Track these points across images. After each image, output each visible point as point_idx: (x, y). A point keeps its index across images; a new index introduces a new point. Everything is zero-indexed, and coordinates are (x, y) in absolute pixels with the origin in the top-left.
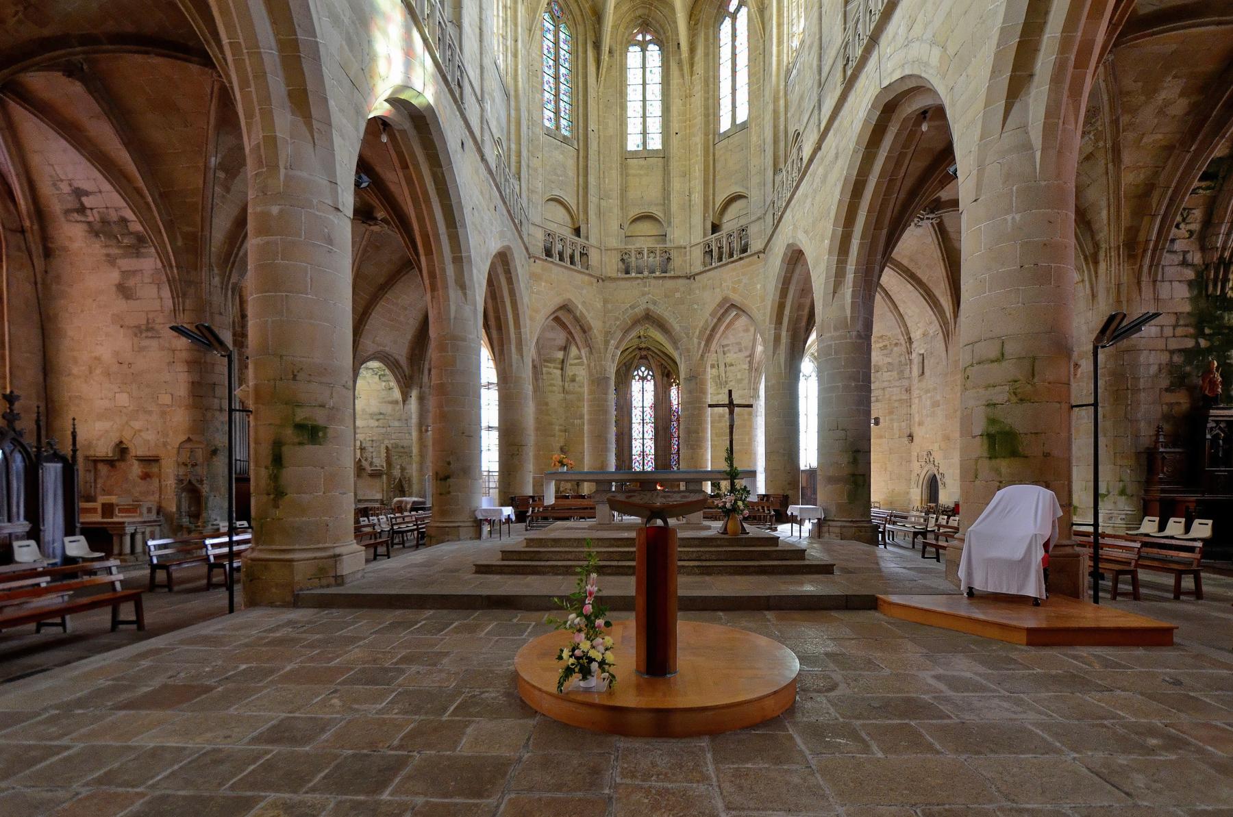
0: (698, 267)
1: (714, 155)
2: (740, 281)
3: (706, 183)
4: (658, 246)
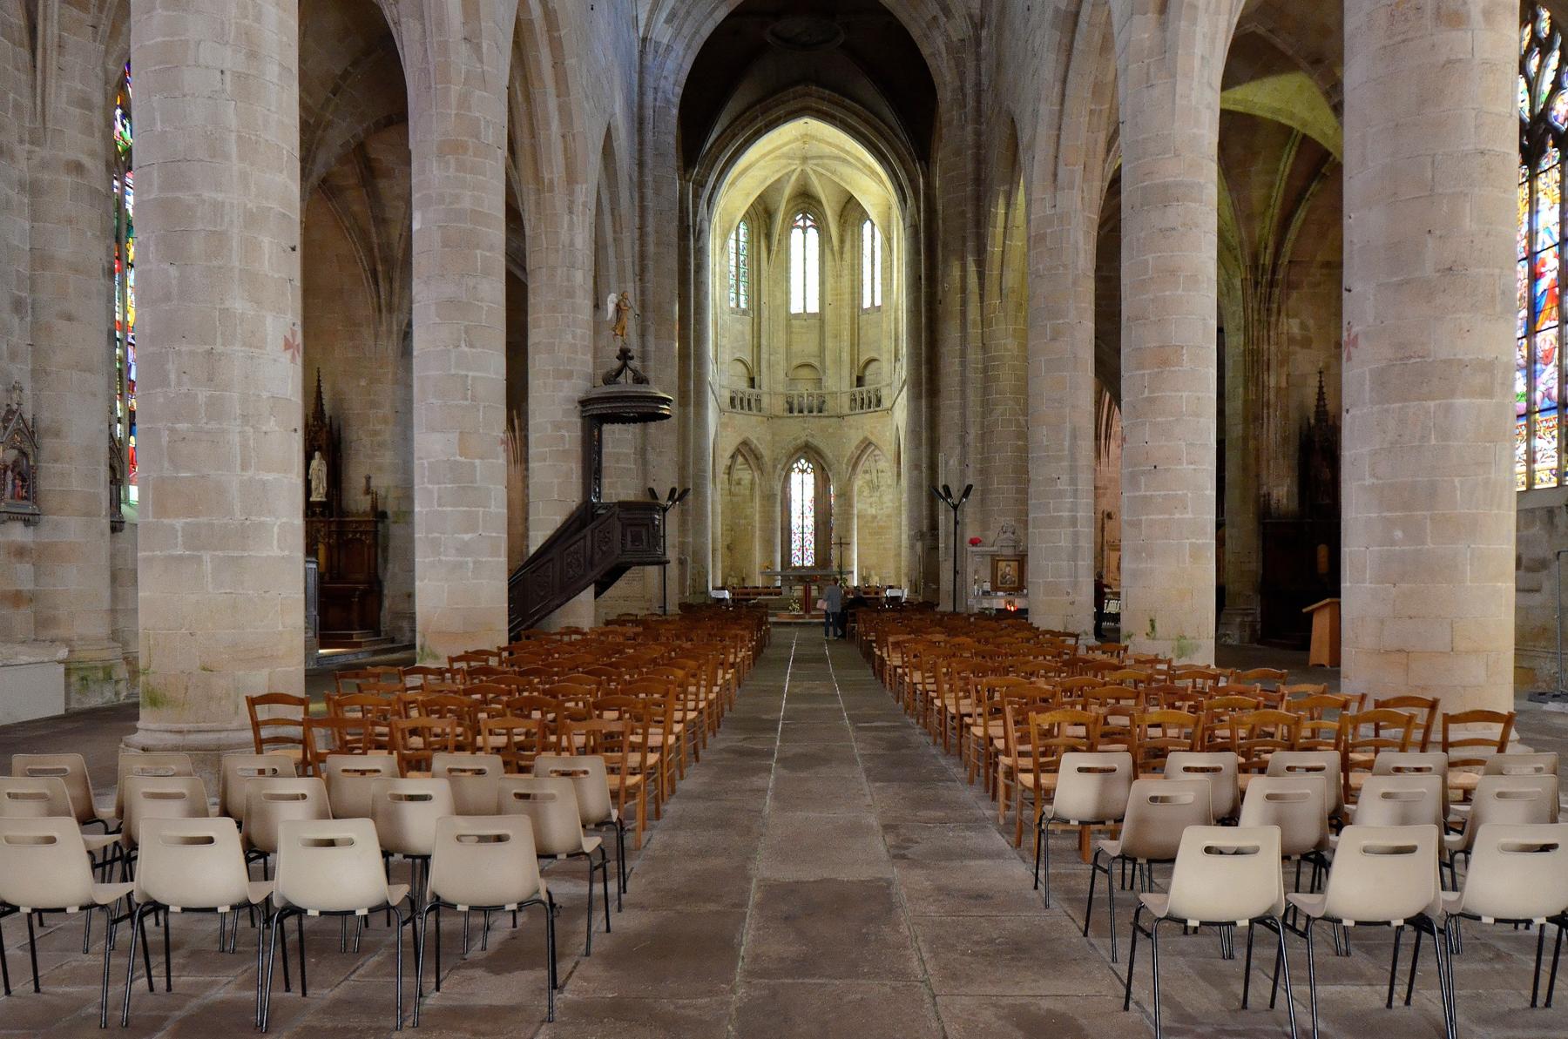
0: (846, 410)
2: (875, 427)
3: (852, 345)
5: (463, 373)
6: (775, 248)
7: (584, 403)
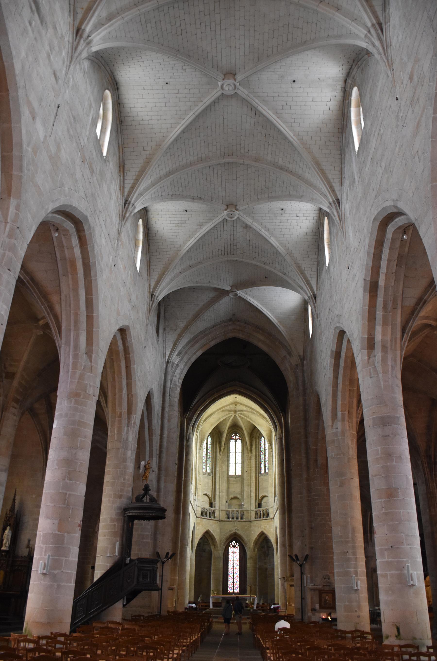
0: (253, 518)
1: (259, 480)
2: (266, 527)
4: (239, 510)
5: (65, 492)
6: (223, 447)
7: (125, 510)
